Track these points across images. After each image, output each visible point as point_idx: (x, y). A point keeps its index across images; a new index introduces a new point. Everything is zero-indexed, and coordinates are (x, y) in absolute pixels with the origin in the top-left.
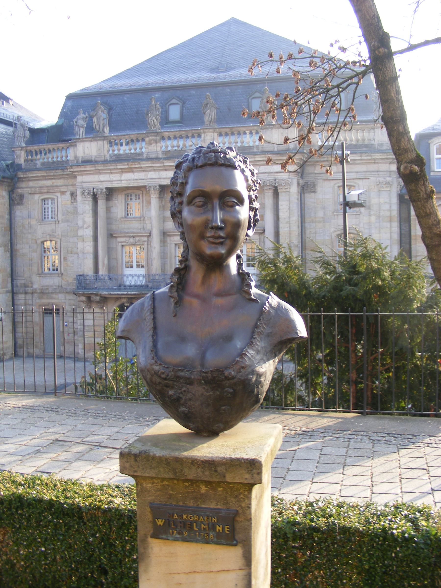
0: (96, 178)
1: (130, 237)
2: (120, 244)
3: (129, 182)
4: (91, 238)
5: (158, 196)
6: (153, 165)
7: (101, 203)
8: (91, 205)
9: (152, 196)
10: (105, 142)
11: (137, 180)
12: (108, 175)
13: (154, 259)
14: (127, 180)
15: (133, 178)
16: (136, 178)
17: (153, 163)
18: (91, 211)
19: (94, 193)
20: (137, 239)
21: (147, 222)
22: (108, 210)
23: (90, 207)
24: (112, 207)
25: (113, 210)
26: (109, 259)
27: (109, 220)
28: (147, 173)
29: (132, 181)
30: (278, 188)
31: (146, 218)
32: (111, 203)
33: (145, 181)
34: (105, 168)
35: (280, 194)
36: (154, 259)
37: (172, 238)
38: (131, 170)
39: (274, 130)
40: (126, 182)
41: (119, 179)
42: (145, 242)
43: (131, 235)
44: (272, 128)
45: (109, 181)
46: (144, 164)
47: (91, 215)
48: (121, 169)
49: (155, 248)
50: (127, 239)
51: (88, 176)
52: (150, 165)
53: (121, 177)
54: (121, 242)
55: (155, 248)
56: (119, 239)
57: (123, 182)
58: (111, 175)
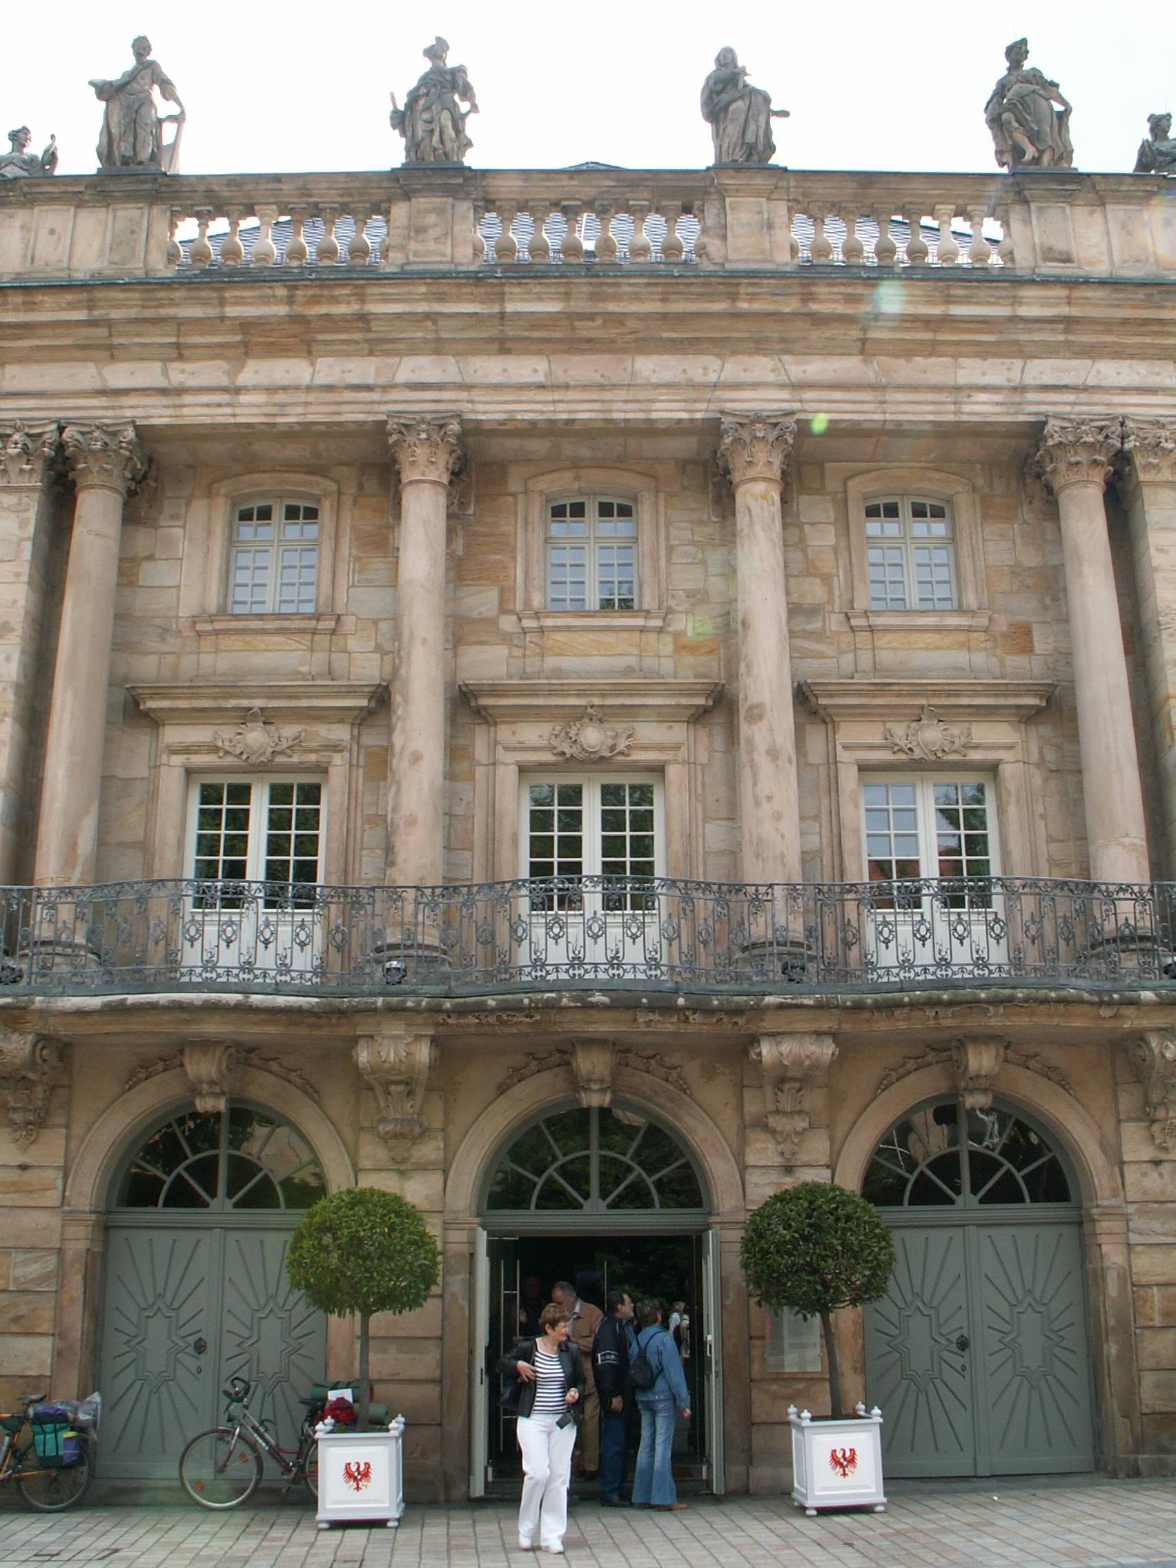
0: (85, 375)
1: (245, 716)
2: (178, 760)
3: (281, 397)
4: (11, 696)
5: (445, 479)
6: (437, 307)
7: (97, 511)
8: (32, 515)
9: (408, 475)
10: (156, 210)
11: (330, 388)
12: (157, 366)
13: (412, 821)
14: (271, 390)
15: (306, 379)
16: (321, 380)
17: (441, 298)
18: (28, 547)
19: (61, 447)
20: (289, 731)
21: (352, 644)
22: (128, 569)
23: (23, 524)
24: (151, 558)
25: (153, 573)
26: (101, 841)
27: (124, 626)
28: (394, 360)
29: (302, 397)
30: (1139, 460)
31: (349, 623)
32: (142, 540)
33: (375, 396)
34: (149, 313)
35: (1146, 492)
36: (412, 821)
37: (504, 733)
38: (300, 337)
39: (1081, 213)
40: (260, 398)
41: (224, 381)
42: (336, 748)
43: (258, 703)
44: (1069, 198)
45: (163, 392)
46: (386, 299)
47: (25, 569)
48: (246, 326)
49: (416, 758)
50: (226, 733)
51: (35, 369)
52: (422, 308)
53: (233, 374)
54: (187, 750)
55: (416, 758)
56: (173, 735)
57: (244, 398)
58: (174, 367)
